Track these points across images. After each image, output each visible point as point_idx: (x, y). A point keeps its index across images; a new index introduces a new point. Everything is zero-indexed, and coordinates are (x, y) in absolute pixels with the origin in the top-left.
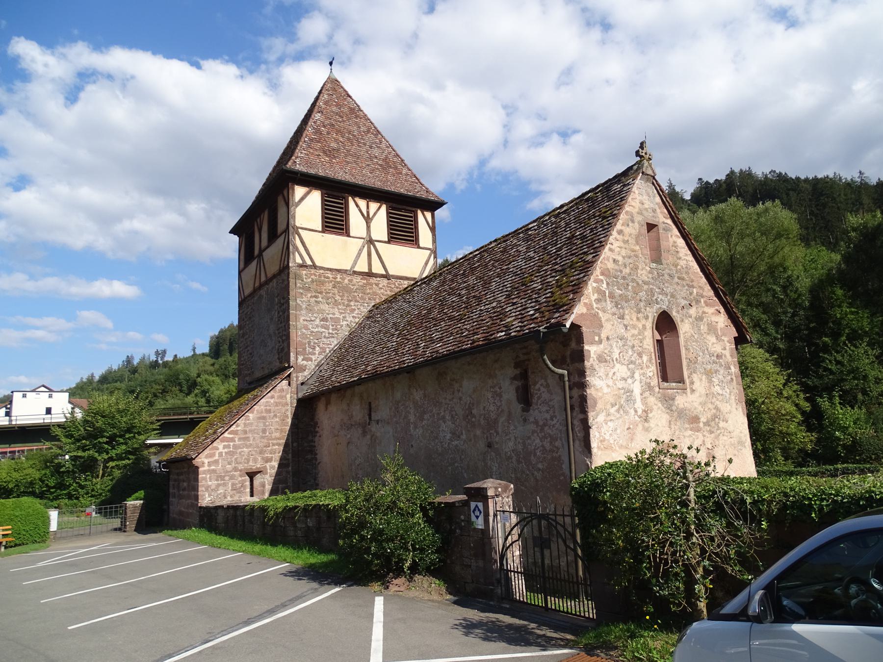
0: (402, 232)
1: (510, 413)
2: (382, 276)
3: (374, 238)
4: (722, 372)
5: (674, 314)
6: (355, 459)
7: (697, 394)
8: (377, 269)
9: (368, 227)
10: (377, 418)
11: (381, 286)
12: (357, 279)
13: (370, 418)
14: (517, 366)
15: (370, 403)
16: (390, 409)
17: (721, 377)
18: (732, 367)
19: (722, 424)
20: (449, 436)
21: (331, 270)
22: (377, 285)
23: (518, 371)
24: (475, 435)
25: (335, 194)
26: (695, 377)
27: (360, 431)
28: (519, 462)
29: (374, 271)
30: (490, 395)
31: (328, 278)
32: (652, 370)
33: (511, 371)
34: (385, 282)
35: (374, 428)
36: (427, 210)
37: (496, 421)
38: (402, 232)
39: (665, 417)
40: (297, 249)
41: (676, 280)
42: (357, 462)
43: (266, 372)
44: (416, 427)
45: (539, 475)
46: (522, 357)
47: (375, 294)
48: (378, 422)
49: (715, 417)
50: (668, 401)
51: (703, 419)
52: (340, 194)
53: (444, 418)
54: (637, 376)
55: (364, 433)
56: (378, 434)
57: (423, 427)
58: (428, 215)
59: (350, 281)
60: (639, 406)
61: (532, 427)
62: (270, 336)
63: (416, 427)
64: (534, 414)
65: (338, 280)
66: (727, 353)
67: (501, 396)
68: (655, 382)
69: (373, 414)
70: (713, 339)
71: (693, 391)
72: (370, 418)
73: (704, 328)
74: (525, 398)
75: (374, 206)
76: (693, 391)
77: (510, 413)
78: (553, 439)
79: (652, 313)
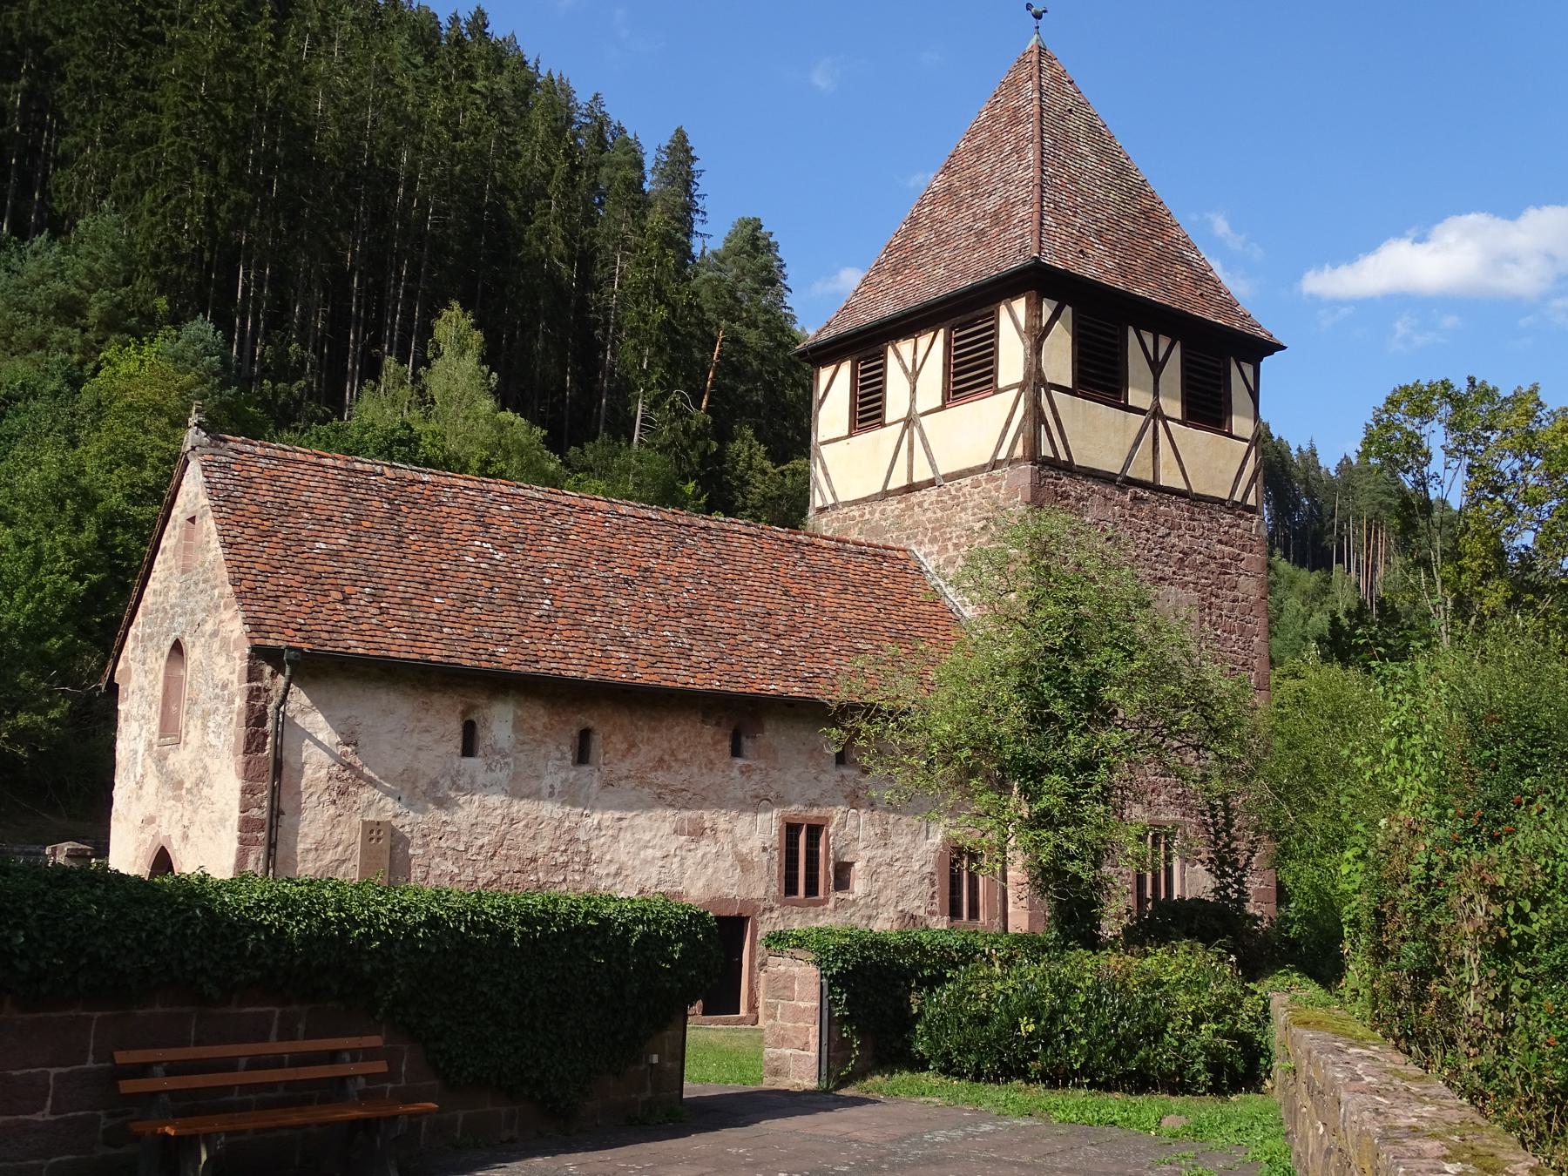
0: (970, 375)
2: (931, 483)
3: (920, 409)
4: (222, 709)
5: (187, 640)
7: (189, 748)
8: (922, 473)
9: (914, 390)
11: (926, 505)
12: (893, 506)
17: (219, 718)
18: (237, 700)
19: (206, 791)
21: (856, 502)
22: (920, 504)
25: (870, 353)
26: (191, 728)
29: (915, 480)
31: (853, 518)
32: (155, 726)
34: (933, 491)
36: (1015, 295)
38: (970, 375)
39: (156, 781)
40: (817, 482)
41: (201, 586)
47: (917, 524)
49: (200, 780)
50: (161, 759)
51: (187, 785)
52: (876, 350)
54: (144, 734)
58: (1020, 306)
59: (883, 512)
60: (139, 770)
65: (867, 516)
66: (235, 678)
68: (155, 739)
70: (221, 660)
71: (186, 744)
73: (216, 646)
75: (924, 341)
76: (186, 744)
79: (167, 647)
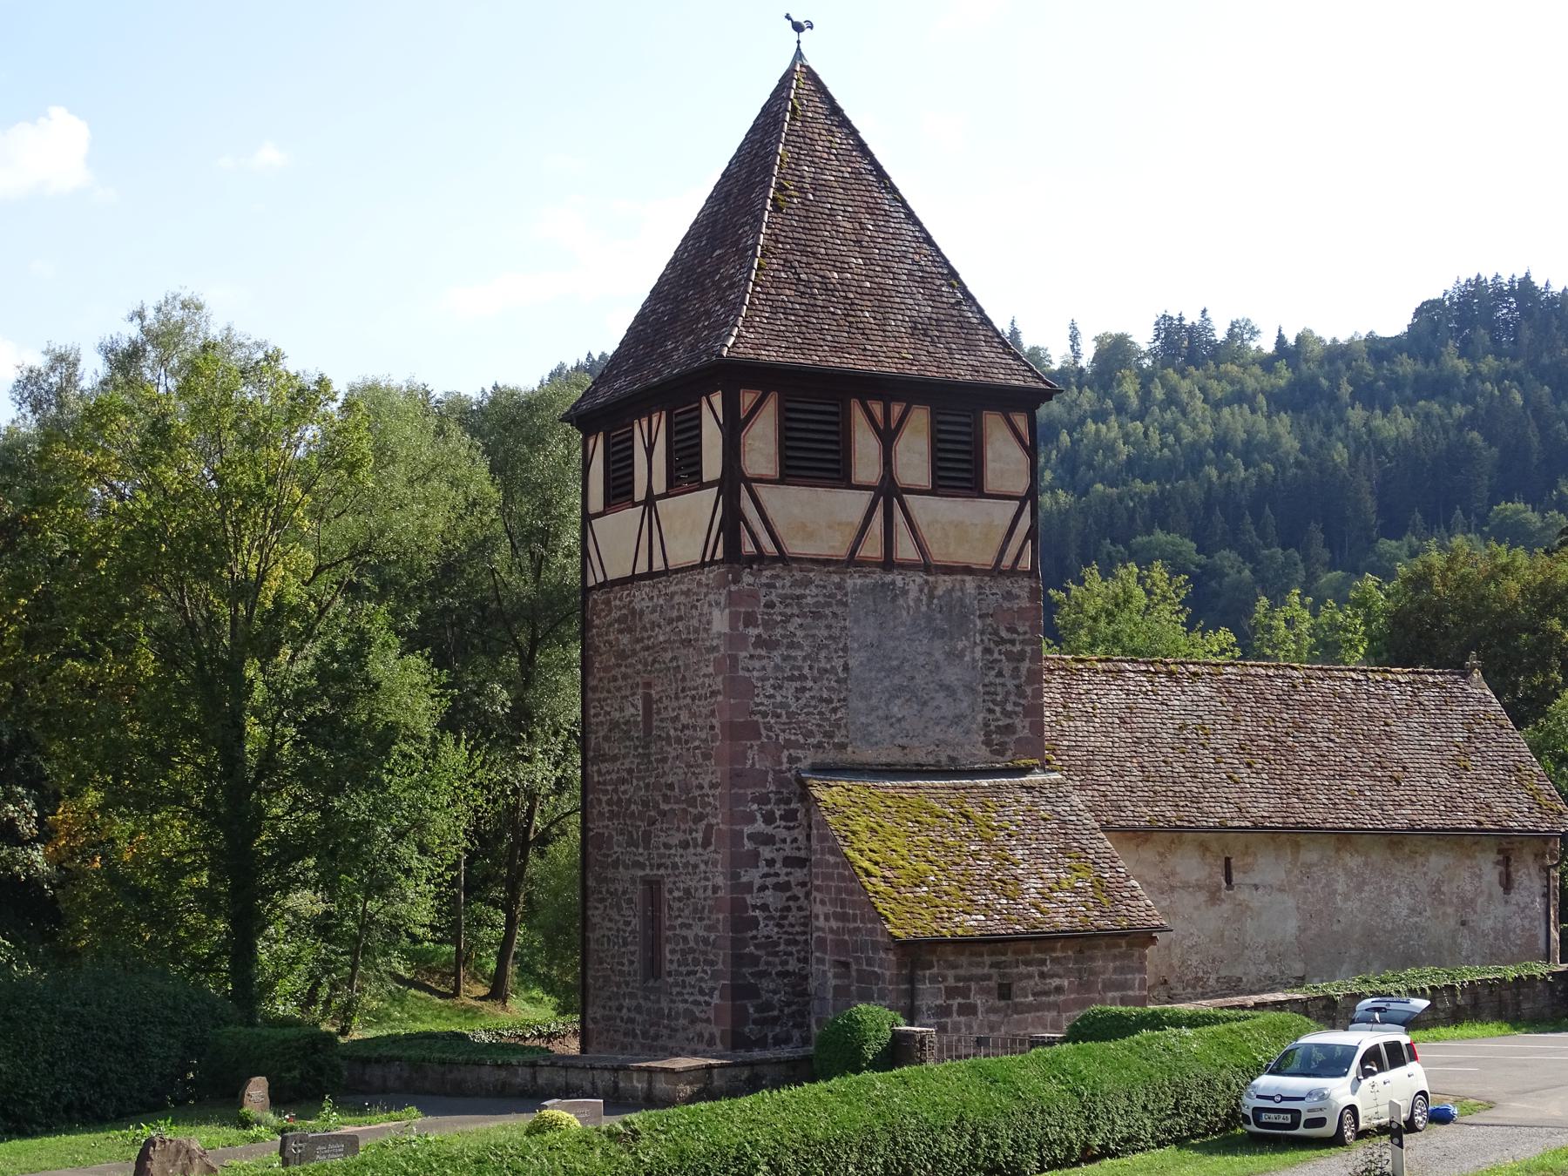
1: (1490, 895)
6: (1184, 938)
10: (1248, 881)
13: (1229, 880)
14: (1500, 852)
15: (1228, 860)
16: (1288, 872)
20: (1405, 912)
23: (1500, 857)
24: (1444, 913)
27: (1202, 897)
28: (1496, 939)
30: (1467, 875)
33: (1493, 856)
35: (1243, 895)
37: (1472, 901)
42: (1187, 943)
43: (920, 756)
44: (1346, 897)
45: (1515, 950)
46: (1505, 846)
48: (1256, 887)
53: (1398, 893)
55: (1214, 898)
56: (1255, 904)
57: (1361, 900)
61: (1514, 908)
62: (949, 690)
63: (1346, 897)
64: (1515, 897)
67: (1480, 877)
69: (1236, 877)
72: (1229, 880)
74: (1507, 884)
77: (1490, 895)
78: (1533, 919)
